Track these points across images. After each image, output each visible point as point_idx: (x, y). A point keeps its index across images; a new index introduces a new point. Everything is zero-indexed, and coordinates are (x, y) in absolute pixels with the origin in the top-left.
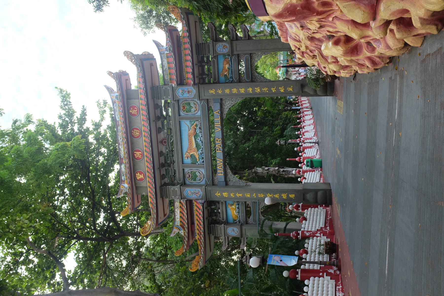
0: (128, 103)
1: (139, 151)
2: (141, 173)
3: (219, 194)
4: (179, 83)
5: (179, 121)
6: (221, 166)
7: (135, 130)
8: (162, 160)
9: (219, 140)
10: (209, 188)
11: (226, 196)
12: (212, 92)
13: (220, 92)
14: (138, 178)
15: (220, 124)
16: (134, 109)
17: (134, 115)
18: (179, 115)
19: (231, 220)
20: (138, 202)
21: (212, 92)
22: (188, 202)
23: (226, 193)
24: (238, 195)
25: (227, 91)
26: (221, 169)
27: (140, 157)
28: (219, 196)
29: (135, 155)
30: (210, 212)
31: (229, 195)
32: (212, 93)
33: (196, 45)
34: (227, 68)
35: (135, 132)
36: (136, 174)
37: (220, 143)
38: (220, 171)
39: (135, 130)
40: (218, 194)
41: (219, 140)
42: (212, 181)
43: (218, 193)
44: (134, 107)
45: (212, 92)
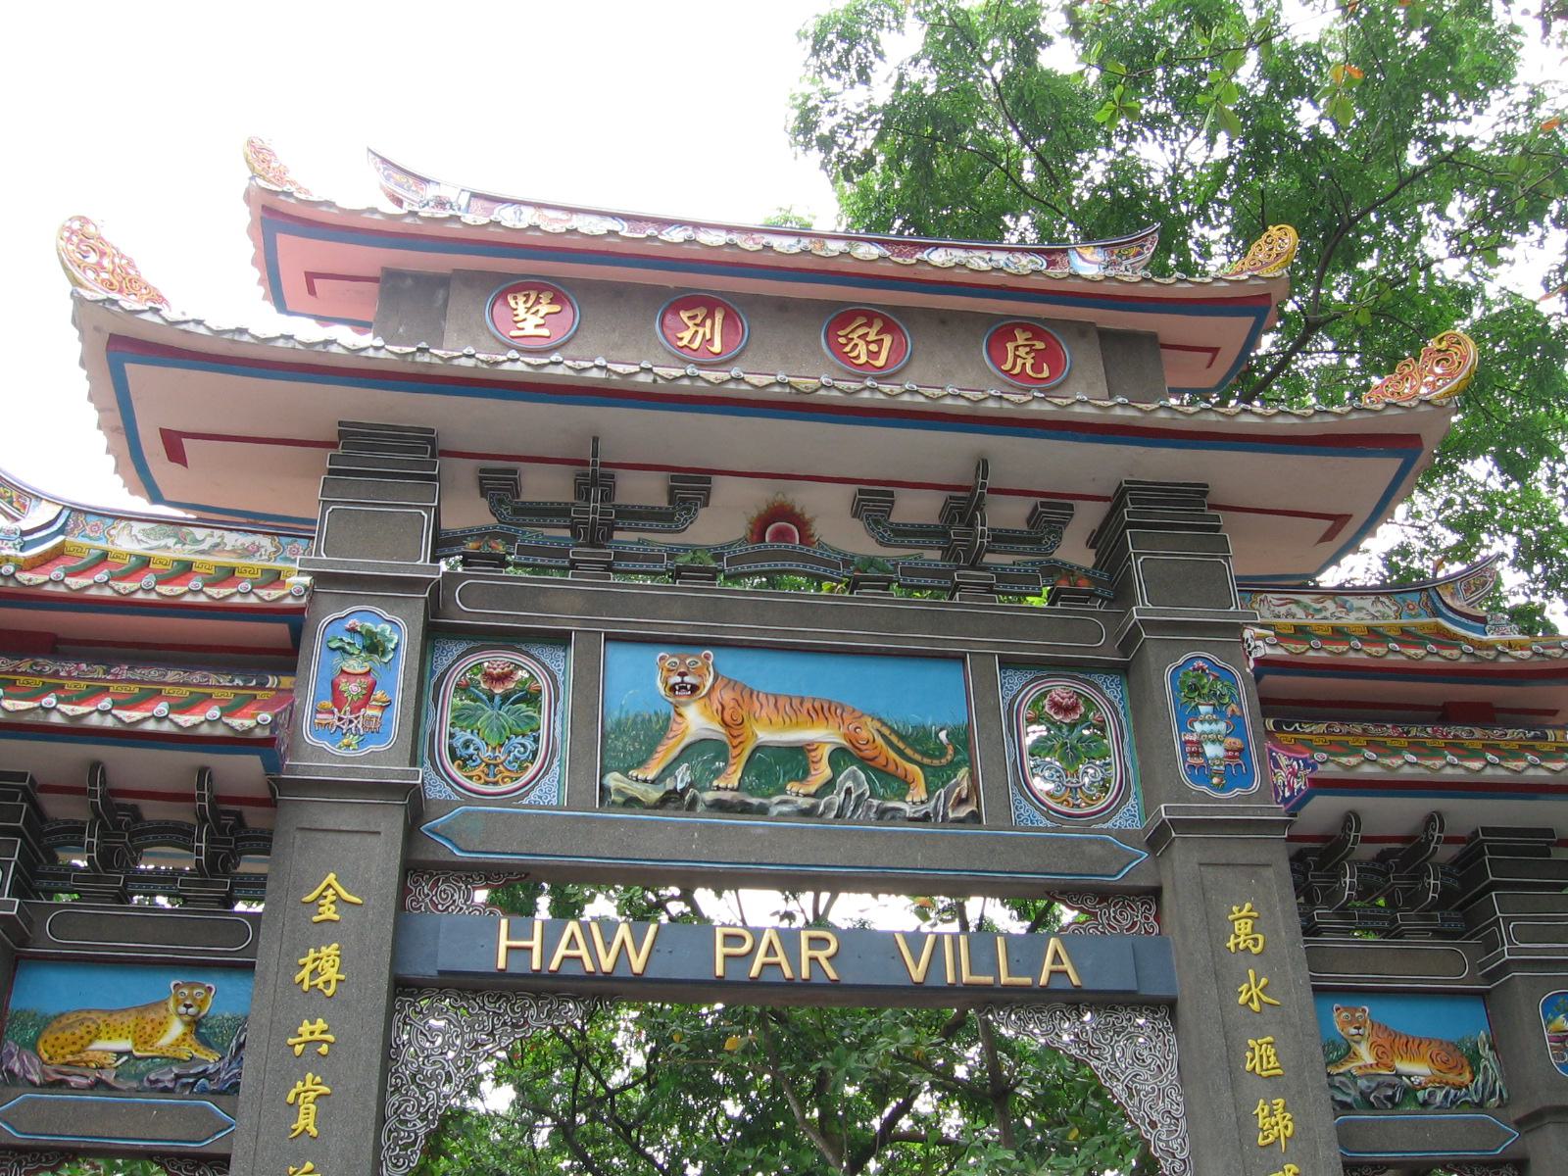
0: (1082, 330)
3: (329, 912)
4: (1273, 681)
5: (960, 658)
6: (583, 951)
7: (887, 340)
8: (644, 490)
9: (821, 955)
10: (391, 823)
11: (305, 973)
12: (1243, 928)
13: (1250, 992)
15: (966, 977)
16: (1040, 358)
18: (1007, 663)
20: (311, 277)
21: (1243, 928)
22: (279, 631)
23: (331, 973)
24: (308, 1089)
25: (1262, 1056)
26: (562, 951)
27: (687, 335)
28: (315, 904)
29: (701, 312)
30: (136, 814)
31: (313, 1001)
32: (1228, 929)
33: (1549, 832)
34: (1404, 1066)
35: (872, 337)
36: (545, 298)
37: (795, 965)
38: (536, 943)
39: (887, 340)
41: (821, 955)
42: (441, 857)
43: (339, 901)
45: (1242, 932)
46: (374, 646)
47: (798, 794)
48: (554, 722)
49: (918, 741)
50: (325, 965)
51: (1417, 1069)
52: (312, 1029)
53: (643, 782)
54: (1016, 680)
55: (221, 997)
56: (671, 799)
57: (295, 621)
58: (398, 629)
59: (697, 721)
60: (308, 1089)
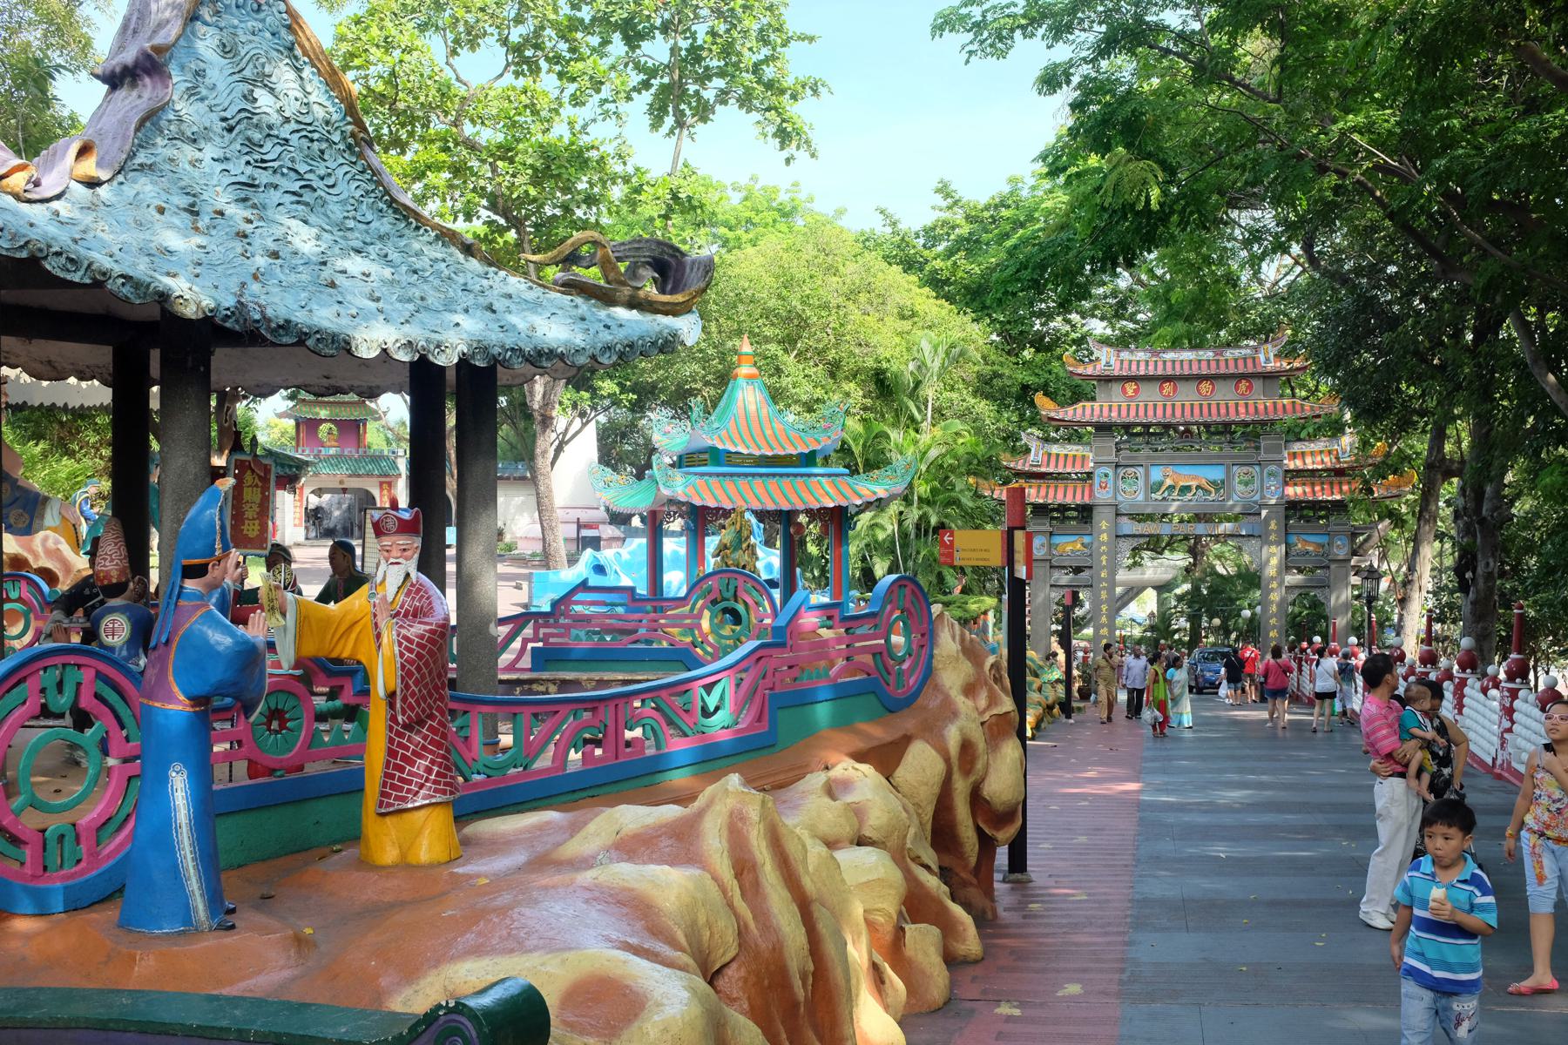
1: (1175, 391)
2: (1136, 391)
14: (1127, 385)
16: (1248, 388)
17: (1237, 388)
19: (1057, 540)
24: (1104, 558)
31: (1103, 543)
40: (1104, 525)
44: (1250, 388)
46: (1106, 475)
47: (1189, 496)
48: (1141, 482)
49: (1214, 483)
50: (1104, 537)
51: (1310, 548)
52: (1103, 548)
53: (1158, 496)
54: (1235, 468)
55: (1087, 539)
56: (1164, 499)
57: (1090, 475)
58: (1110, 472)
59: (1169, 482)
60: (1104, 558)
